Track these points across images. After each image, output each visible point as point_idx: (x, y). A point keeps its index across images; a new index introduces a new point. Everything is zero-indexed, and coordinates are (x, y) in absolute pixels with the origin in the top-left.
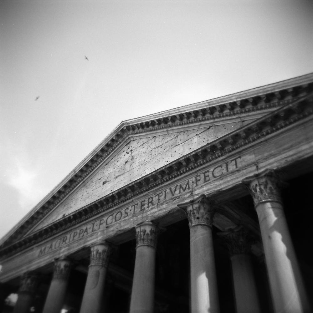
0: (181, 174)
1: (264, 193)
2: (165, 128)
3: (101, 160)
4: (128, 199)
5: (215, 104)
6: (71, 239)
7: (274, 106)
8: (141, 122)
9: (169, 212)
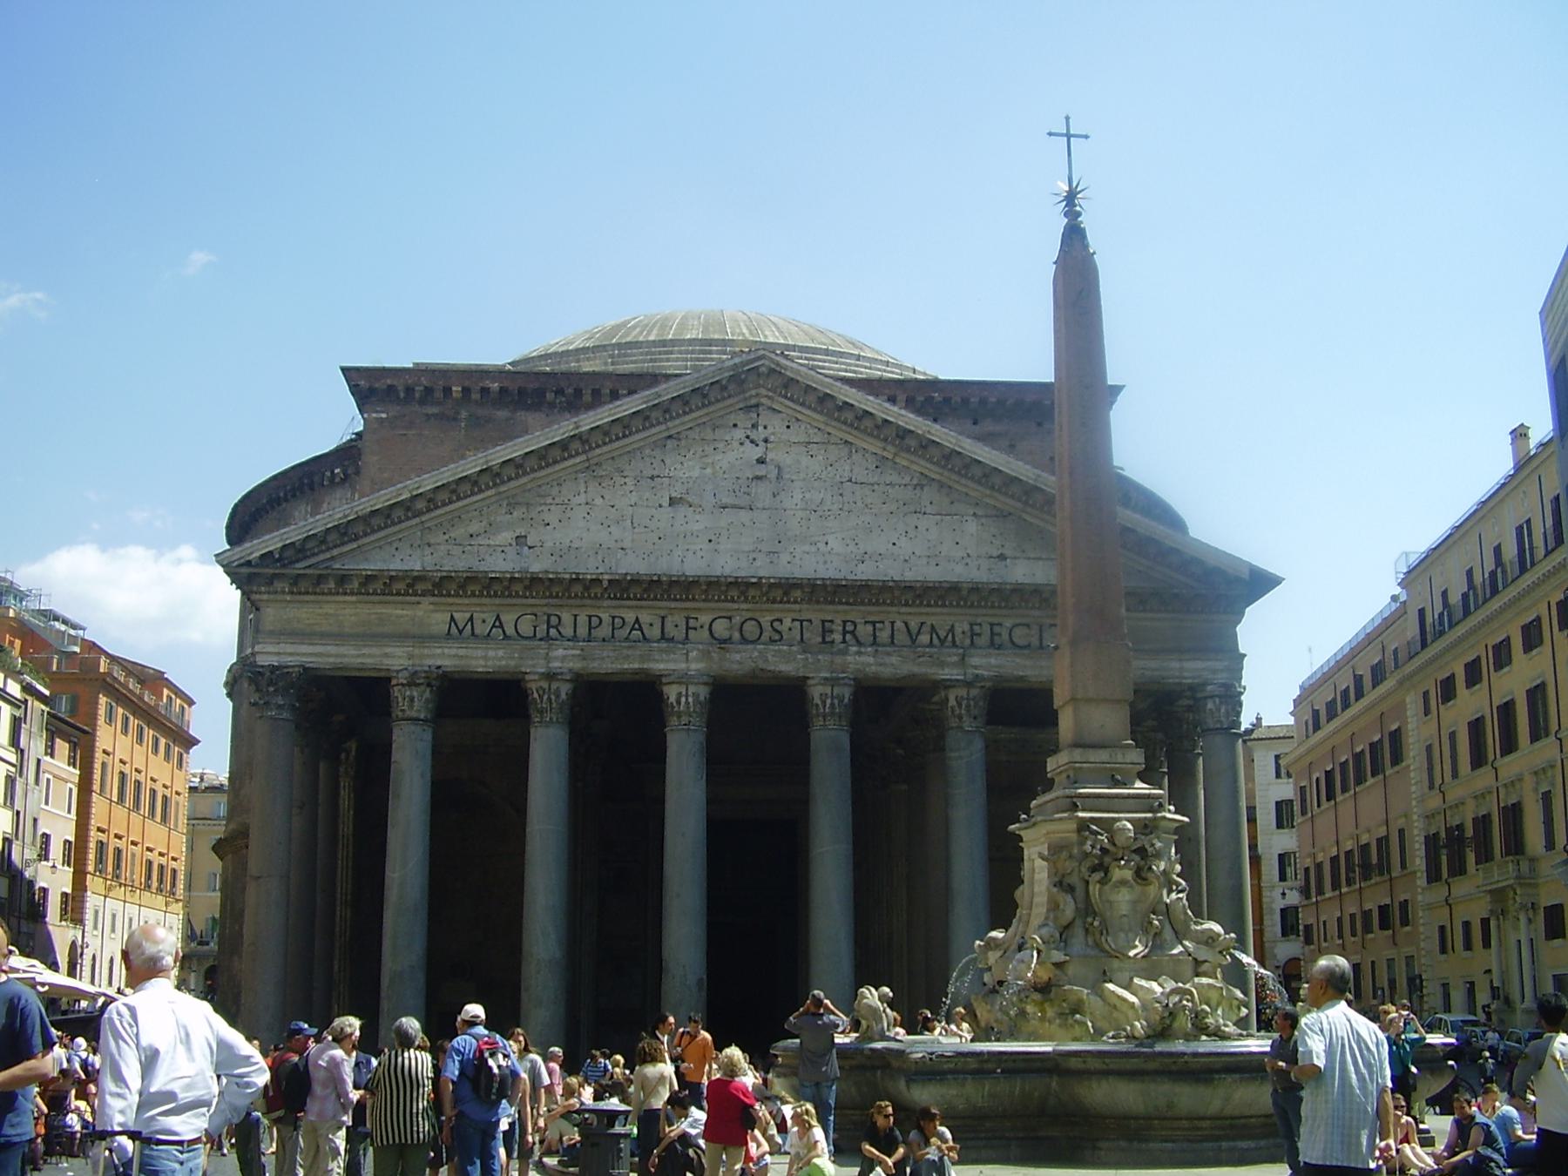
0: (944, 606)
2: (893, 445)
3: (661, 419)
4: (788, 602)
5: (1049, 487)
6: (582, 631)
8: (828, 391)
9: (904, 678)
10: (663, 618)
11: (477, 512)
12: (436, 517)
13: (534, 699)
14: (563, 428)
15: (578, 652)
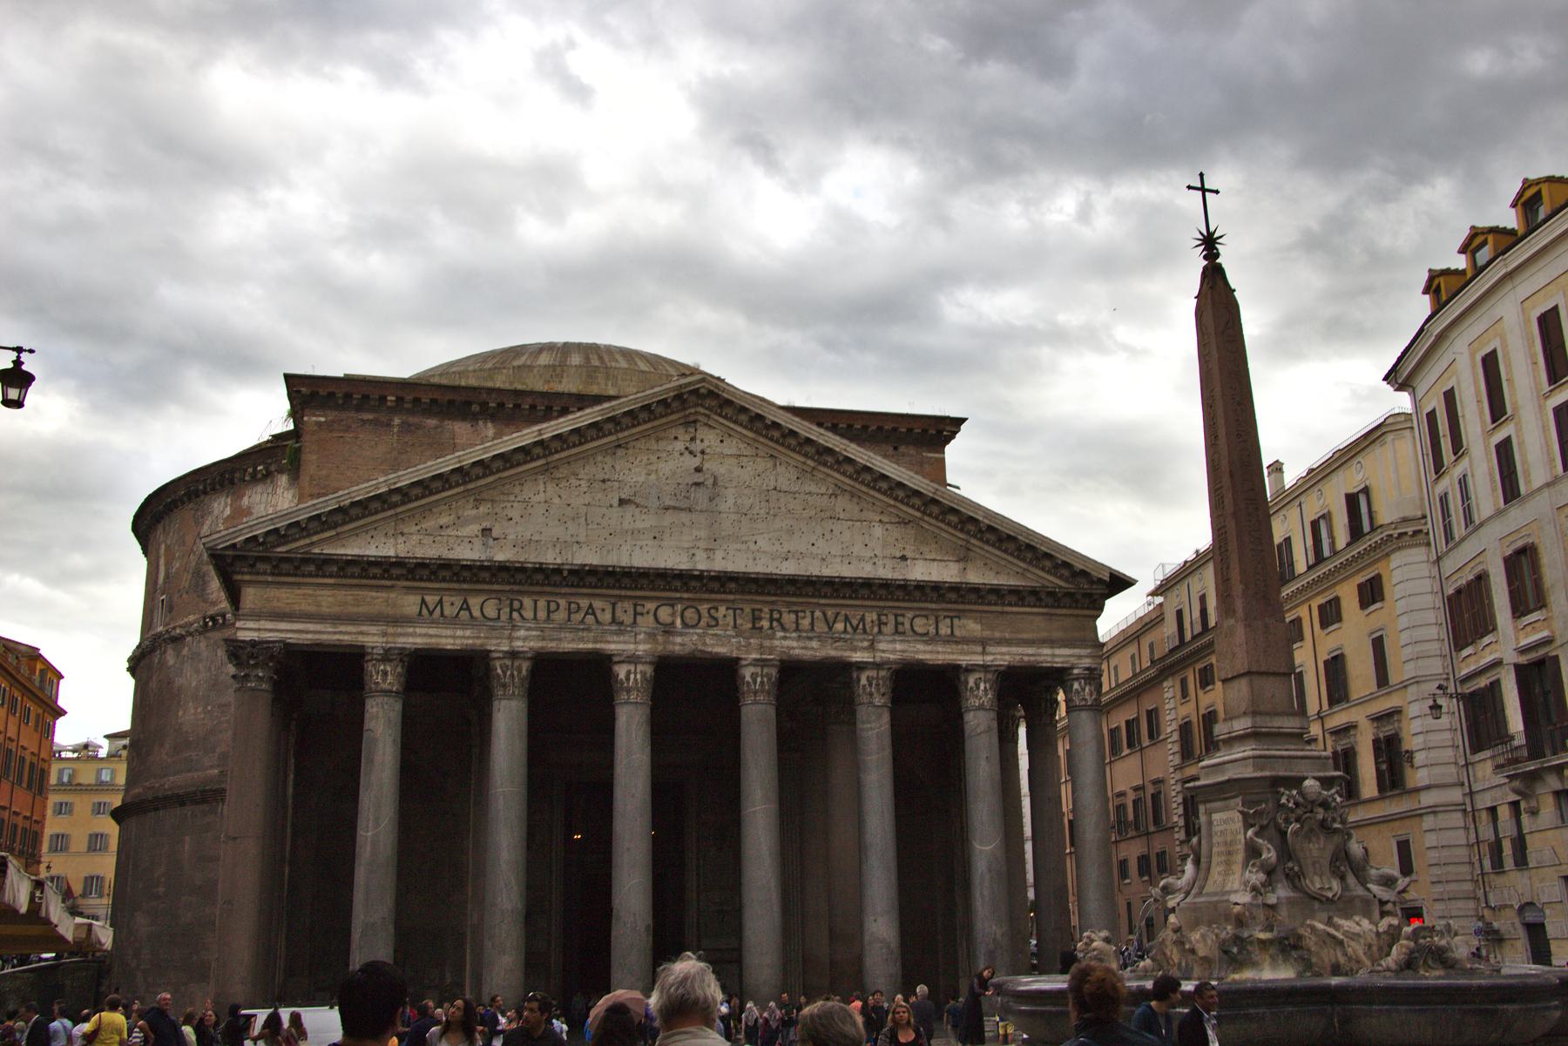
0: (857, 598)
1: (989, 696)
2: (812, 458)
4: (724, 592)
6: (542, 614)
7: (1024, 560)
8: (759, 412)
10: (614, 605)
11: (445, 507)
12: (409, 510)
13: (498, 674)
14: (526, 436)
15: (538, 633)
